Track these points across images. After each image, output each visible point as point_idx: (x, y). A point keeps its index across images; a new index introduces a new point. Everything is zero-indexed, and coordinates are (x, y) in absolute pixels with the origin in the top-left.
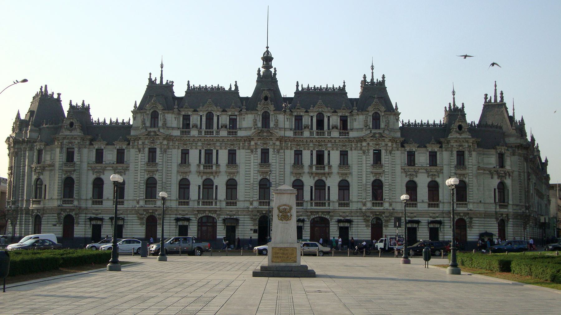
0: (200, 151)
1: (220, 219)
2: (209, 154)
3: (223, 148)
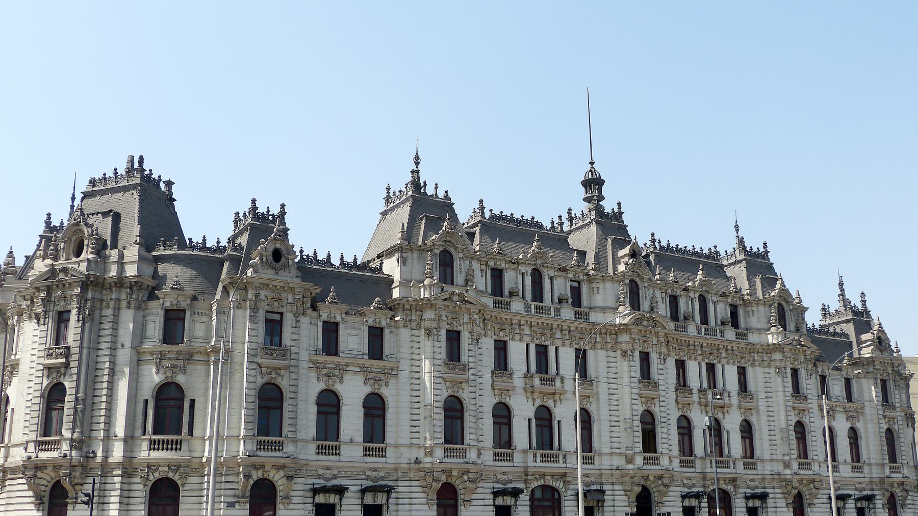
0: (527, 345)
2: (542, 352)
3: (567, 343)
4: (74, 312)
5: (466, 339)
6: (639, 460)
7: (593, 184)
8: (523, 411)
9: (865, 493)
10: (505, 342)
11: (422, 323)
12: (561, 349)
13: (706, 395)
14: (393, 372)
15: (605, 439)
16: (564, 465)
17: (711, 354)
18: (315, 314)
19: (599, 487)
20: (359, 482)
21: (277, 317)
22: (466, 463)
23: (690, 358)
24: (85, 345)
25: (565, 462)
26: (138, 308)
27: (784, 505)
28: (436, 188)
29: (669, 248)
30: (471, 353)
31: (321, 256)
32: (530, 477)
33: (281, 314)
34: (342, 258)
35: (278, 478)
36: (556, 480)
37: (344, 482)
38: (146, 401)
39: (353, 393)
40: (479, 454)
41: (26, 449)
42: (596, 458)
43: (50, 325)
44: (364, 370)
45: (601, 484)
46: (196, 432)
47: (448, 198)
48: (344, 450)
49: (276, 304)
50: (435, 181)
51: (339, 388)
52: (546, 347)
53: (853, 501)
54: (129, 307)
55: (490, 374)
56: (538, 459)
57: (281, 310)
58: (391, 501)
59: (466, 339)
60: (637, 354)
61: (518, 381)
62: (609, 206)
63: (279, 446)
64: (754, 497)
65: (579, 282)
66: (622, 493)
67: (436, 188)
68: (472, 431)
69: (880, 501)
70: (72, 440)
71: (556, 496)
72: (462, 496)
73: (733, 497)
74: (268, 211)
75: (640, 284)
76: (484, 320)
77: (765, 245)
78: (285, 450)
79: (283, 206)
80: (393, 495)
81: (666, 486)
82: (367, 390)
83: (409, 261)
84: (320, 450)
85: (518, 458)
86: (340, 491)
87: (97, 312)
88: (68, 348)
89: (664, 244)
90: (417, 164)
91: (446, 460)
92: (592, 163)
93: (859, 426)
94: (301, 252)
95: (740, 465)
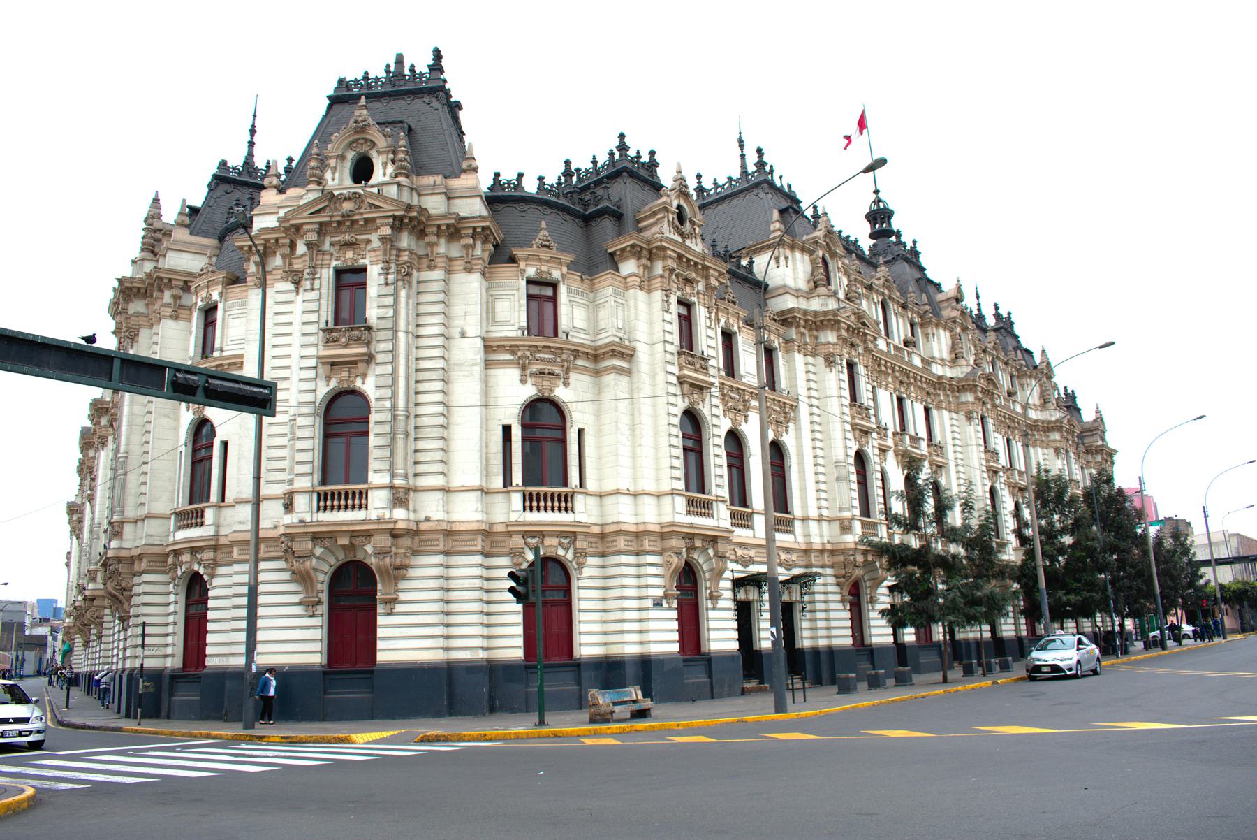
4: (374, 274)
24: (402, 325)
26: (483, 274)
38: (507, 430)
41: (289, 507)
43: (324, 291)
46: (591, 485)
54: (469, 270)
58: (806, 598)
70: (392, 487)
79: (652, 153)
87: (415, 273)
88: (369, 328)
92: (876, 192)
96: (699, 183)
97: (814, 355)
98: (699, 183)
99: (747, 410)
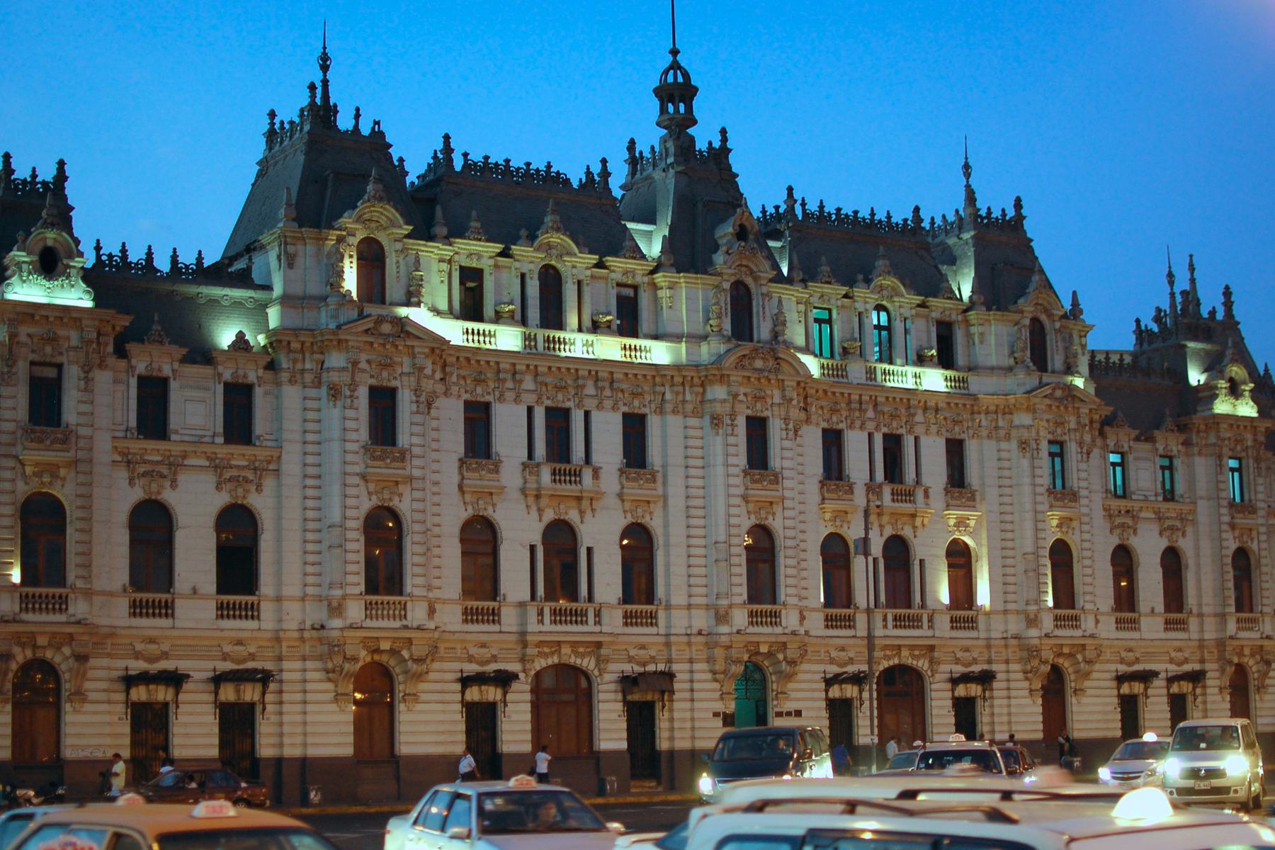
0: (530, 410)
1: (607, 677)
3: (608, 403)
5: (407, 403)
6: (740, 618)
7: (677, 93)
8: (520, 532)
9: (1187, 668)
10: (487, 406)
11: (324, 375)
12: (596, 416)
13: (879, 495)
14: (269, 468)
15: (678, 579)
16: (597, 629)
17: (893, 417)
18: (122, 364)
19: (661, 667)
20: (210, 665)
21: (51, 373)
22: (406, 627)
23: (851, 427)
25: (598, 622)
27: (1026, 693)
28: (357, 116)
29: (822, 215)
30: (416, 429)
31: (136, 255)
32: (531, 651)
33: (60, 367)
34: (174, 258)
35: (61, 659)
36: (583, 656)
37: (183, 665)
39: (196, 507)
40: (432, 612)
42: (661, 614)
44: (218, 467)
45: (669, 661)
47: (381, 135)
48: (181, 606)
49: (48, 349)
50: (355, 106)
51: (169, 496)
52: (567, 412)
53: (1164, 683)
55: (457, 465)
56: (547, 618)
57: (58, 360)
58: (269, 697)
59: (407, 403)
60: (741, 422)
61: (511, 476)
62: (703, 136)
63: (61, 604)
64: (966, 678)
65: (635, 288)
66: (709, 676)
67: (357, 116)
68: (417, 570)
69: (1214, 681)
71: (584, 684)
72: (401, 687)
73: (927, 680)
74: (34, 176)
75: (753, 290)
76: (444, 365)
77: (1018, 204)
78: (71, 610)
79: (61, 164)
80: (272, 686)
81: (792, 663)
82: (223, 499)
83: (300, 261)
84: (137, 609)
85: (509, 618)
86: (175, 680)
89: (813, 207)
90: (325, 68)
91: (369, 623)
92: (674, 52)
93: (1185, 545)
94: (98, 248)
95: (943, 623)
96: (272, 124)
97: (318, 384)
98: (272, 124)
99: (175, 473)
